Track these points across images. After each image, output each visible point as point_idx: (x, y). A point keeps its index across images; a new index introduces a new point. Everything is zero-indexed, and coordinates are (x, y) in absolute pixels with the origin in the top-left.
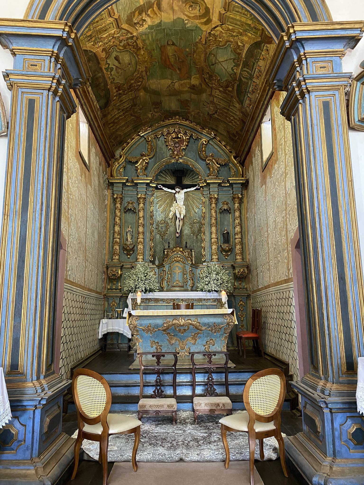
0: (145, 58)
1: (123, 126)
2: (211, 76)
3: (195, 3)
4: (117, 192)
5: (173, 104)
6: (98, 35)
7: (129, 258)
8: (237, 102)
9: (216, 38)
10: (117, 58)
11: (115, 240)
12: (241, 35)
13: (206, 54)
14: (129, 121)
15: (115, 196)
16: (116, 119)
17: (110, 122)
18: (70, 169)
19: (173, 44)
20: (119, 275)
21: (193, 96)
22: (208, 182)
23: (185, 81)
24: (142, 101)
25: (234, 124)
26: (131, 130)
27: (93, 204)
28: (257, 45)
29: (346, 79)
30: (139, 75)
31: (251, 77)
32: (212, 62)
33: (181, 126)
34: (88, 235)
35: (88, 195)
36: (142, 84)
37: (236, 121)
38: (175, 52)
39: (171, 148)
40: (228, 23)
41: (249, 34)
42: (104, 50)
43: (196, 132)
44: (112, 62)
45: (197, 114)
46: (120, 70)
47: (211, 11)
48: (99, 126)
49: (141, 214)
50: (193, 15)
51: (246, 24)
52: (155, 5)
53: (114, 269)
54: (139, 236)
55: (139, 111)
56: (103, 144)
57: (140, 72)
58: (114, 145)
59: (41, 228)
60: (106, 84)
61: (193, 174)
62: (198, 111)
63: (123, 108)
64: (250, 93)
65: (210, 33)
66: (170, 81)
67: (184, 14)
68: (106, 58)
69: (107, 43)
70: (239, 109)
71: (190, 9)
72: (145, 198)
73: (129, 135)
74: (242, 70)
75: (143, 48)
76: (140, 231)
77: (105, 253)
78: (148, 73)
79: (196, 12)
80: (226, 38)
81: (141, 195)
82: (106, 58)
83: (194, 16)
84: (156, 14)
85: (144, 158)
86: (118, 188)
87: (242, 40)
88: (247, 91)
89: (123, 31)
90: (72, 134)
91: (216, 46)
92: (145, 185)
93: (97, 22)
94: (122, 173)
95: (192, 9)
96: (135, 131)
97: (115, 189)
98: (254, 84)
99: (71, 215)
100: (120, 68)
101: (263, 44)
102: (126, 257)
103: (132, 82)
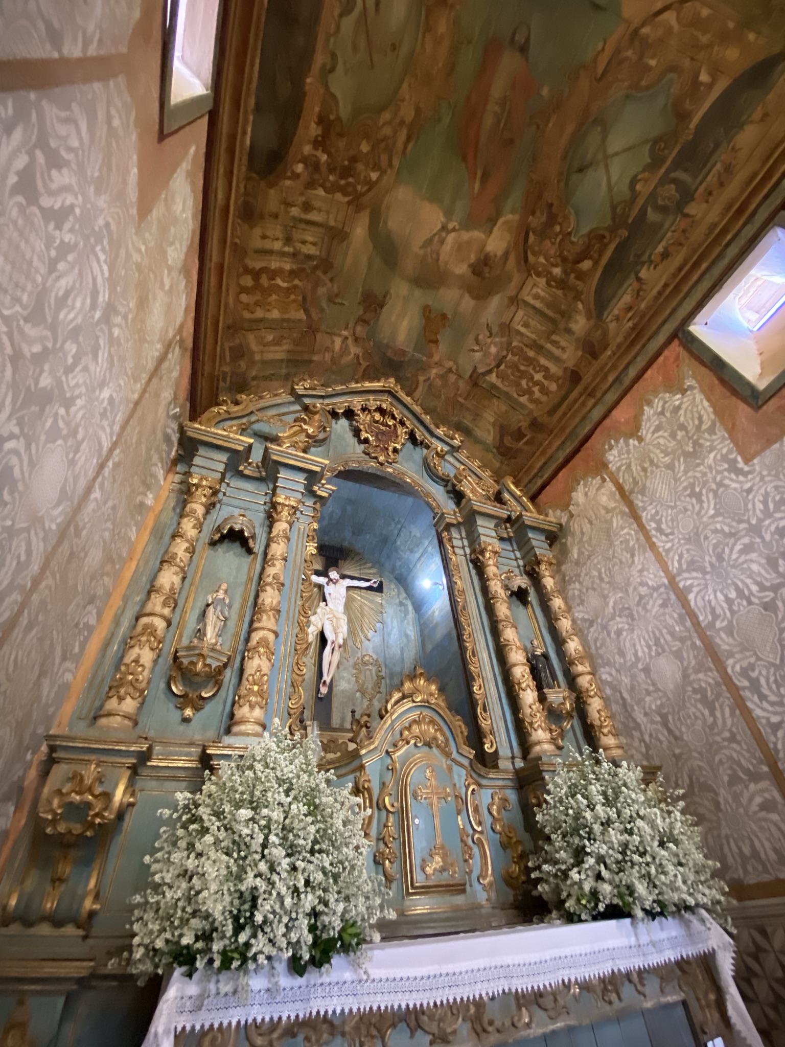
2: (552, 219)
4: (204, 472)
7: (186, 720)
11: (144, 620)
14: (288, 320)
20: (110, 815)
21: (468, 303)
22: (475, 508)
23: (477, 234)
25: (537, 394)
26: (282, 360)
30: (387, 131)
33: (395, 403)
37: (546, 383)
39: (366, 441)
43: (421, 428)
45: (442, 377)
49: (277, 549)
53: (90, 772)
54: (259, 620)
55: (324, 304)
60: (306, 56)
61: (361, 559)
62: (451, 364)
63: (298, 245)
64: (651, 262)
70: (578, 340)
74: (662, 182)
78: (410, 146)
81: (287, 498)
85: (305, 427)
86: (208, 467)
88: (645, 258)
96: (287, 377)
97: (197, 460)
102: (176, 715)
103: (365, 148)
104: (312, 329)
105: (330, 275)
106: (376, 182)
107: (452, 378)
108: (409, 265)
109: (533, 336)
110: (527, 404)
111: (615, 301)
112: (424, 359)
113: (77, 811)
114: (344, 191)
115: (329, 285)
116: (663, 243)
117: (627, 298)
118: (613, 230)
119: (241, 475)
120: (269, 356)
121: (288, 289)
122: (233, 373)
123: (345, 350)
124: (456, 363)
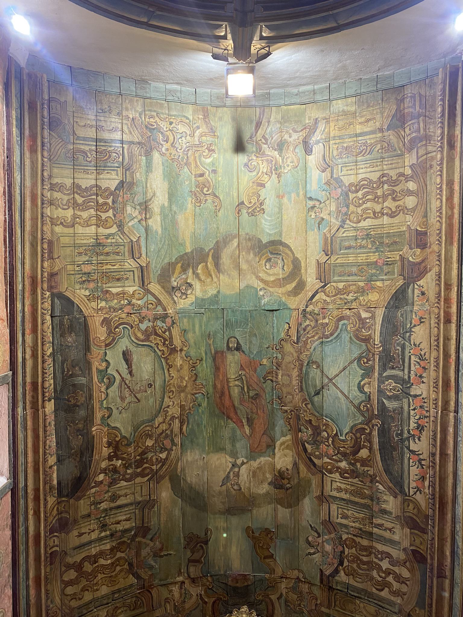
0: (182, 378)
3: (275, 254)
5: (234, 549)
8: (389, 489)
9: (317, 321)
10: (127, 356)
12: (363, 291)
13: (302, 365)
14: (119, 591)
17: (70, 560)
19: (238, 348)
21: (283, 513)
23: (262, 459)
24: (162, 526)
25: (396, 585)
28: (399, 299)
30: (164, 427)
31: (406, 383)
32: (315, 386)
36: (169, 462)
38: (242, 368)
40: (336, 278)
41: (379, 284)
42: (106, 322)
44: (115, 357)
45: (294, 589)
46: (127, 393)
47: (303, 264)
50: (272, 279)
51: (369, 264)
52: (210, 259)
57: (169, 418)
60: (89, 420)
65: (304, 310)
67: (258, 278)
68: (106, 345)
69: (115, 310)
70: (397, 517)
71: (267, 267)
74: (381, 381)
75: (181, 350)
78: (184, 428)
79: (278, 270)
80: (335, 313)
82: (106, 345)
83: (273, 281)
84: (211, 276)
87: (366, 304)
88: (406, 435)
89: (150, 297)
91: (319, 338)
93: (107, 254)
95: (271, 266)
98: (418, 402)
100: (129, 387)
101: (412, 285)
103: (149, 443)
104: (146, 588)
105: (149, 536)
106: (167, 458)
107: (305, 588)
108: (218, 503)
109: (357, 525)
110: (392, 598)
111: (406, 473)
112: (267, 576)
115: (152, 544)
116: (412, 420)
117: (414, 470)
118: (368, 422)
121: (112, 564)
123: (185, 595)
124: (300, 571)
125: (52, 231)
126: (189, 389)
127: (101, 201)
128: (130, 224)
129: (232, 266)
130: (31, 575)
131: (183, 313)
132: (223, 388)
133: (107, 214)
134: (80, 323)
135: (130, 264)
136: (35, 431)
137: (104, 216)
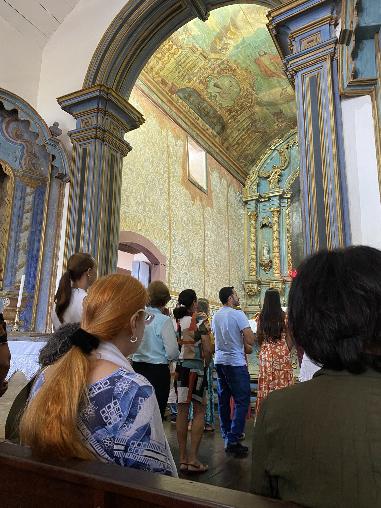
0: (244, 76)
1: (250, 145)
4: (250, 210)
6: (190, 73)
7: (267, 274)
10: (216, 86)
14: (254, 139)
15: (249, 214)
16: (239, 139)
17: (234, 144)
18: (173, 196)
19: (265, 54)
27: (216, 224)
29: (331, 46)
34: (207, 252)
35: (206, 216)
42: (200, 83)
48: (220, 151)
49: (275, 227)
52: (231, 27)
53: (250, 285)
56: (232, 166)
58: (246, 165)
59: (89, 244)
60: (215, 112)
63: (243, 128)
66: (280, 89)
67: (262, 23)
68: (206, 89)
69: (201, 76)
72: (278, 211)
73: (261, 151)
75: (238, 68)
76: (275, 244)
77: (244, 270)
78: (254, 88)
82: (206, 89)
89: (212, 60)
90: (176, 165)
92: (278, 197)
93: (184, 62)
94: (256, 190)
96: (266, 146)
97: (248, 206)
99: (174, 236)
102: (264, 273)
103: (242, 101)
104: (264, 132)
106: (252, 100)
113: (251, 291)
114: (245, 110)
119: (262, 202)
120: (256, 149)
122: (248, 162)
125: (160, 76)
126: (249, 77)
127: (167, 47)
128: (185, 43)
129: (245, 24)
130: (224, 158)
131: (231, 56)
132: (265, 69)
133: (173, 49)
134: (192, 92)
135: (195, 56)
136: (201, 132)
137: (172, 51)
